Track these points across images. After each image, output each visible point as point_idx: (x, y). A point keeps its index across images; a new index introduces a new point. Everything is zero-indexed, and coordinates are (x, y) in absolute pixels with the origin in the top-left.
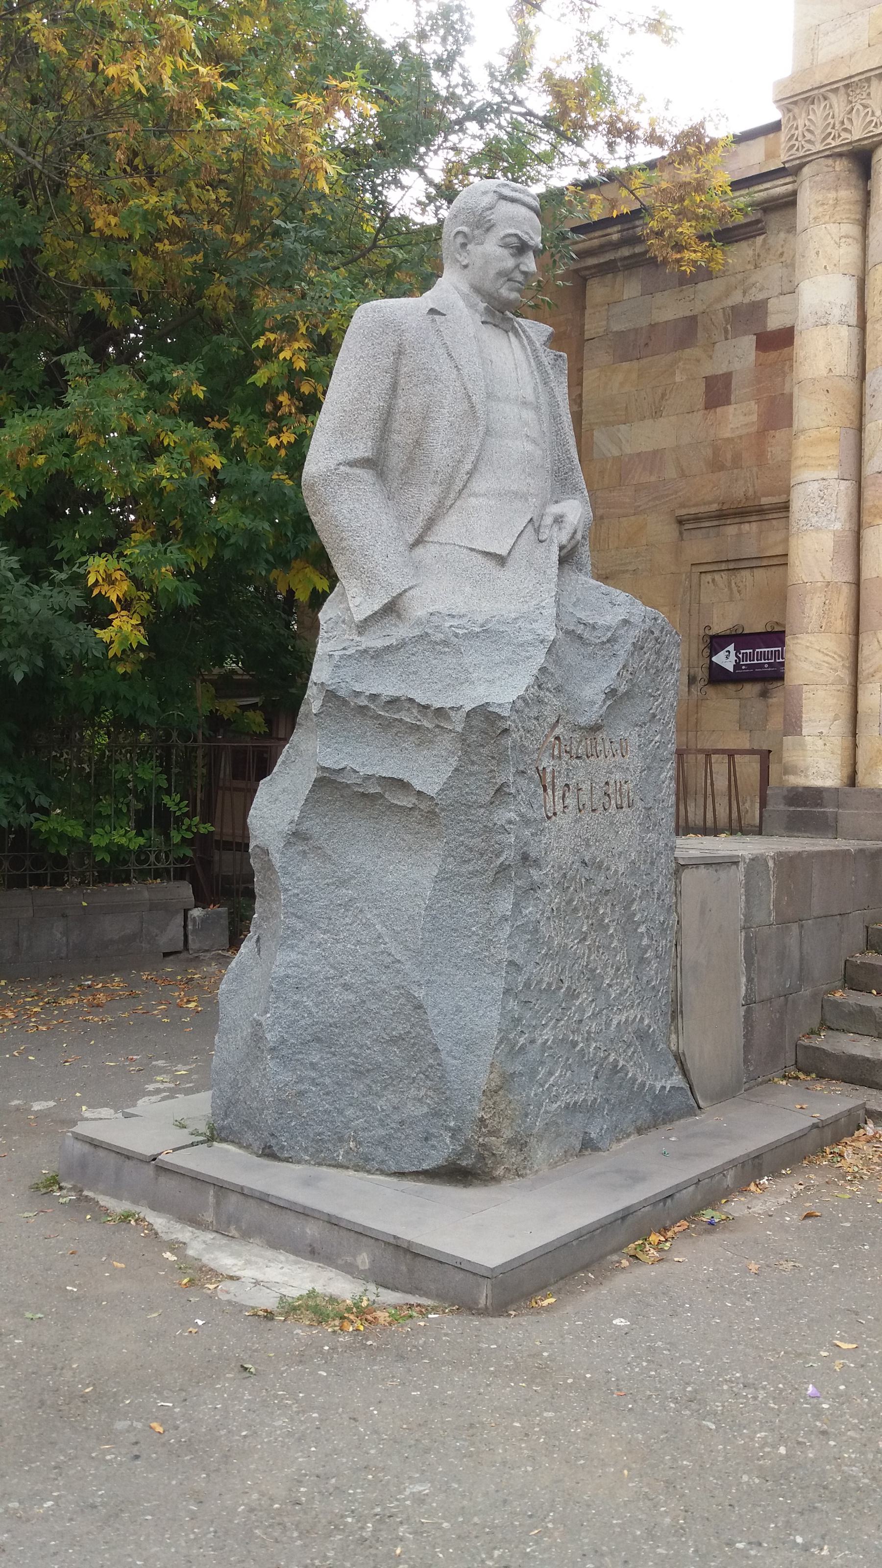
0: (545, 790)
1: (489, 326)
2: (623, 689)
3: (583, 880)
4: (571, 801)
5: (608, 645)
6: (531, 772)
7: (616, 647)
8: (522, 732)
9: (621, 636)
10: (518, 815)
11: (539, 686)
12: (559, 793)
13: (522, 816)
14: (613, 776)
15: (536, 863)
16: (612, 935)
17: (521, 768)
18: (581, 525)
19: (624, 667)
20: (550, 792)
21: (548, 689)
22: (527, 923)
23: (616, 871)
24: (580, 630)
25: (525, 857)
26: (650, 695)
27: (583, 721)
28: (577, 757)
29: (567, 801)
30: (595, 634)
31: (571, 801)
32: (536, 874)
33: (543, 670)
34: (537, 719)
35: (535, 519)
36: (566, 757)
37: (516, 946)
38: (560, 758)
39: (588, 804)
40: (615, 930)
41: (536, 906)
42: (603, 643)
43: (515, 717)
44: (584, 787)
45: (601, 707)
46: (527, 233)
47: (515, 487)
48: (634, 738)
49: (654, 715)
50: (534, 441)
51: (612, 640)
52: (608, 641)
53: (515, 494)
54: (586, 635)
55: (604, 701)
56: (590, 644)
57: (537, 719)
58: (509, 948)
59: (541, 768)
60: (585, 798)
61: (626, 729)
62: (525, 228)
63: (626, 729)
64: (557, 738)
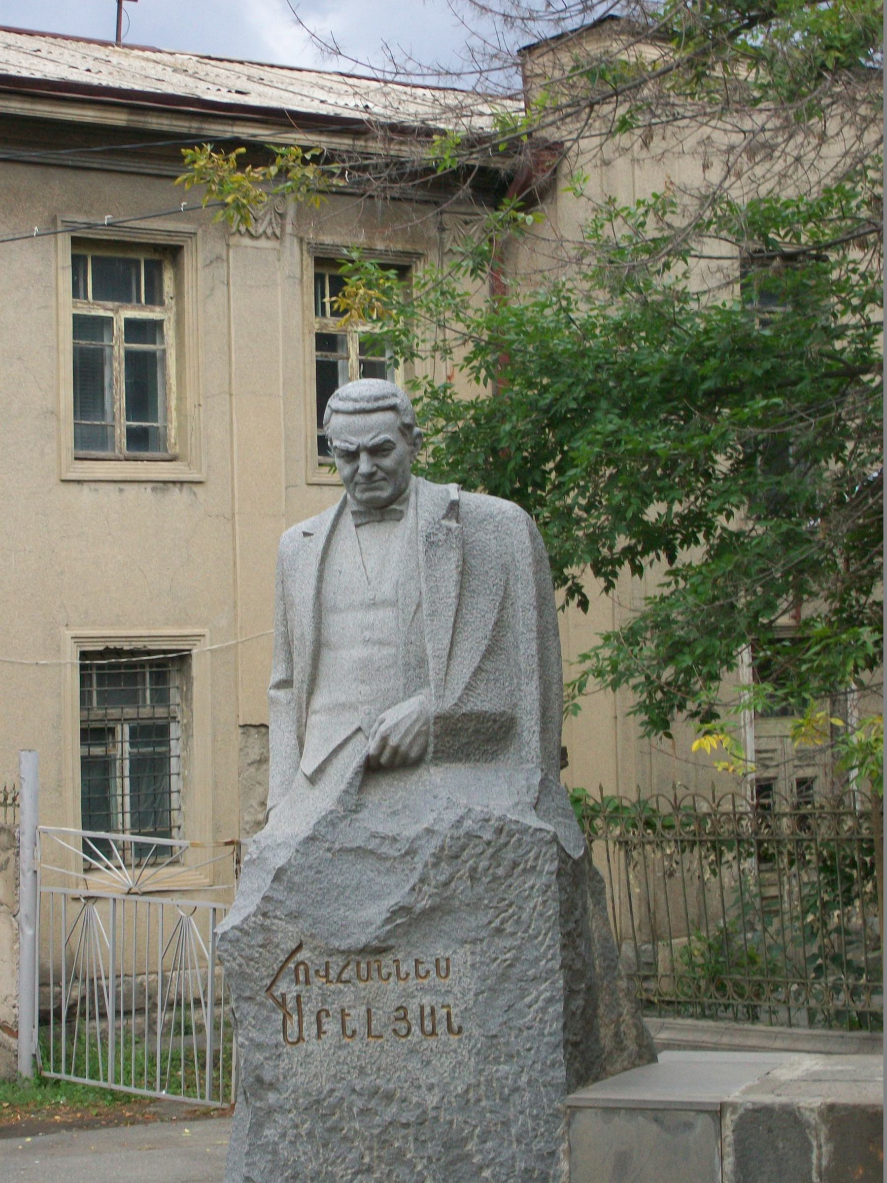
0: (287, 1015)
1: (367, 526)
2: (424, 903)
3: (355, 1110)
4: (331, 1026)
5: (408, 858)
6: (261, 997)
7: (416, 859)
8: (240, 960)
9: (421, 847)
10: (247, 1039)
11: (265, 915)
12: (309, 1020)
13: (251, 1040)
14: (416, 1001)
15: (272, 1086)
16: (420, 1173)
17: (247, 994)
18: (402, 729)
19: (422, 880)
20: (295, 1017)
21: (275, 917)
22: (268, 1144)
23: (419, 1105)
24: (373, 844)
25: (259, 1080)
26: (487, 907)
27: (344, 945)
28: (341, 982)
29: (324, 1028)
30: (398, 846)
31: (331, 1026)
32: (272, 1097)
33: (266, 899)
34: (262, 946)
35: (364, 727)
36: (318, 982)
37: (254, 1164)
38: (307, 982)
39: (362, 1030)
40: (426, 1167)
41: (275, 1128)
42: (404, 856)
43: (227, 946)
44: (352, 1012)
45: (379, 928)
46: (346, 441)
47: (343, 699)
48: (461, 957)
49: (499, 931)
50: (381, 643)
51: (411, 852)
52: (407, 853)
53: (343, 705)
54: (384, 849)
55: (387, 921)
56: (386, 859)
57: (262, 946)
58: (247, 1164)
59: (277, 994)
60: (351, 1025)
61: (446, 948)
62: (343, 437)
63: (446, 948)
64: (302, 963)
